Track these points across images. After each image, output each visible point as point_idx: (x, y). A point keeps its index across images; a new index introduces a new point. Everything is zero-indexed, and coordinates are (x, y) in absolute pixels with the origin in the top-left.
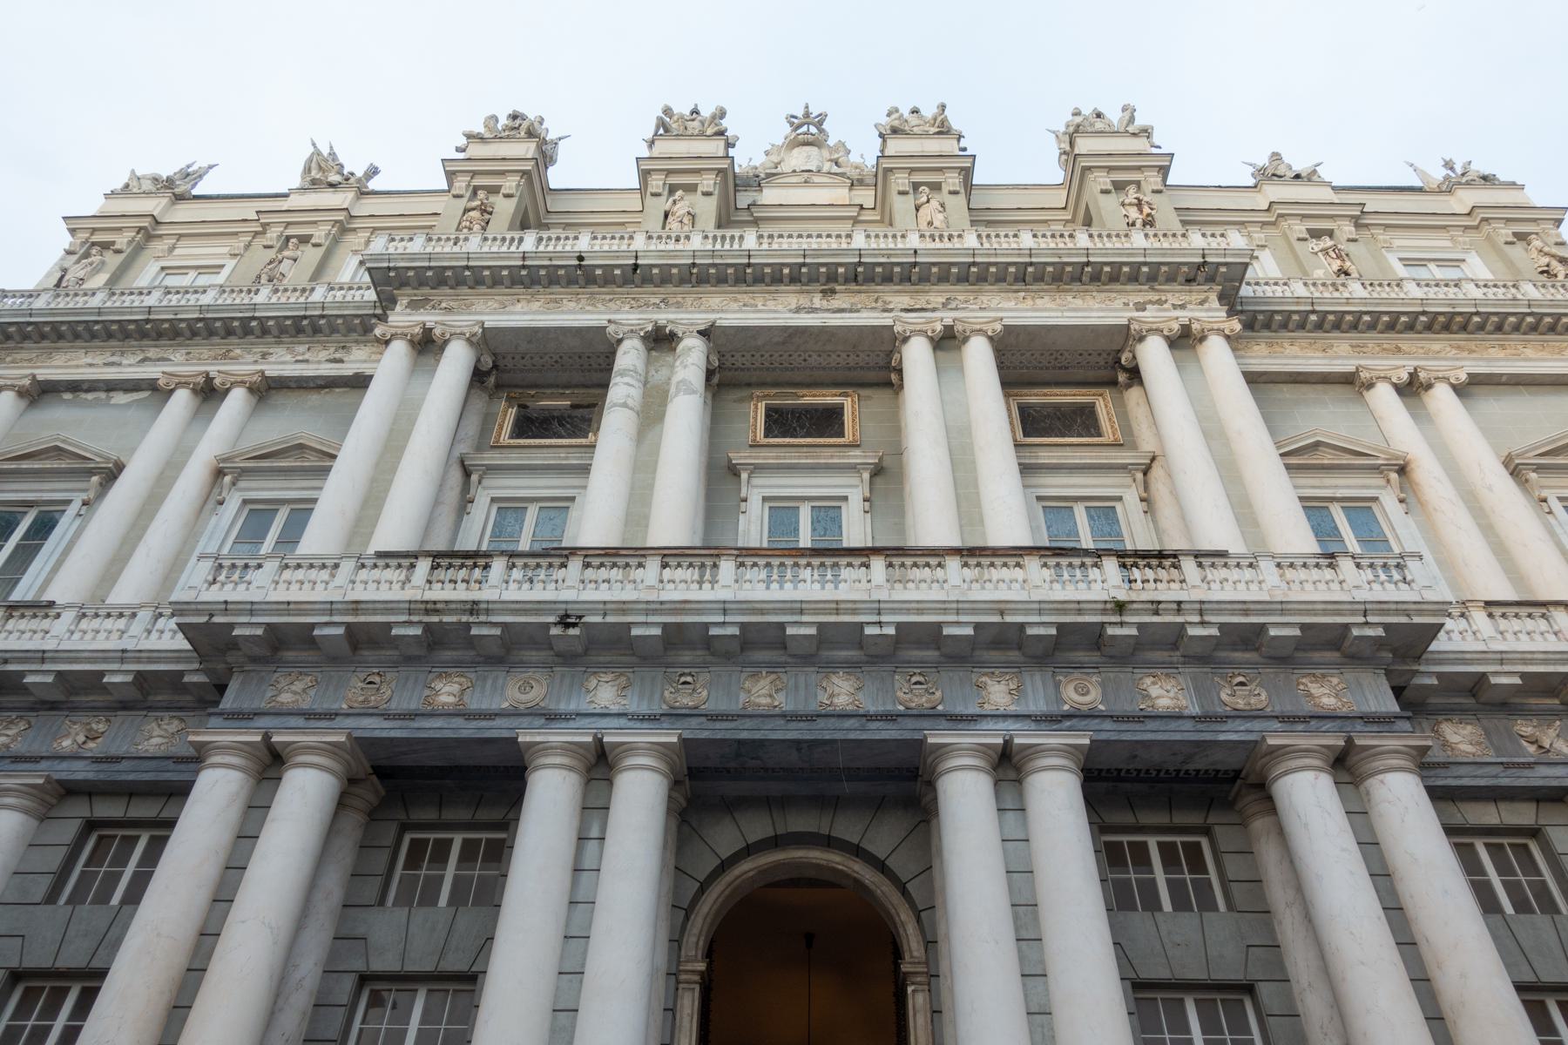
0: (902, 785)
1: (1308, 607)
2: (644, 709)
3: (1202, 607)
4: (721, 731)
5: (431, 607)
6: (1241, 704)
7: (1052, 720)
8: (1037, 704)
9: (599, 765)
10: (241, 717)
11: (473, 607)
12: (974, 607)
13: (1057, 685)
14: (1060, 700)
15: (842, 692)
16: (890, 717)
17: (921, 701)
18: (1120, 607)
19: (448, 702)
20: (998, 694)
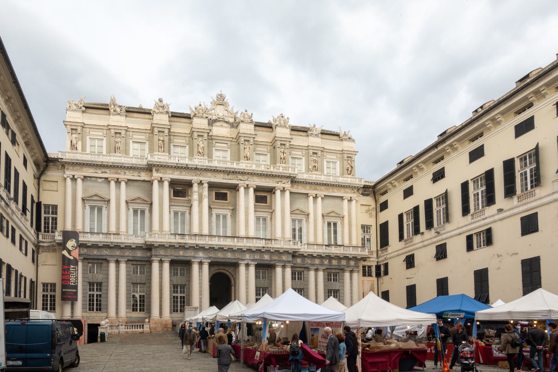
0: (235, 265)
2: (205, 256)
3: (273, 248)
4: (215, 260)
5: (180, 243)
7: (253, 260)
8: (252, 258)
9: (201, 263)
10: (156, 256)
11: (185, 243)
12: (247, 247)
15: (229, 255)
16: (235, 259)
17: (239, 257)
18: (264, 247)
19: (182, 254)
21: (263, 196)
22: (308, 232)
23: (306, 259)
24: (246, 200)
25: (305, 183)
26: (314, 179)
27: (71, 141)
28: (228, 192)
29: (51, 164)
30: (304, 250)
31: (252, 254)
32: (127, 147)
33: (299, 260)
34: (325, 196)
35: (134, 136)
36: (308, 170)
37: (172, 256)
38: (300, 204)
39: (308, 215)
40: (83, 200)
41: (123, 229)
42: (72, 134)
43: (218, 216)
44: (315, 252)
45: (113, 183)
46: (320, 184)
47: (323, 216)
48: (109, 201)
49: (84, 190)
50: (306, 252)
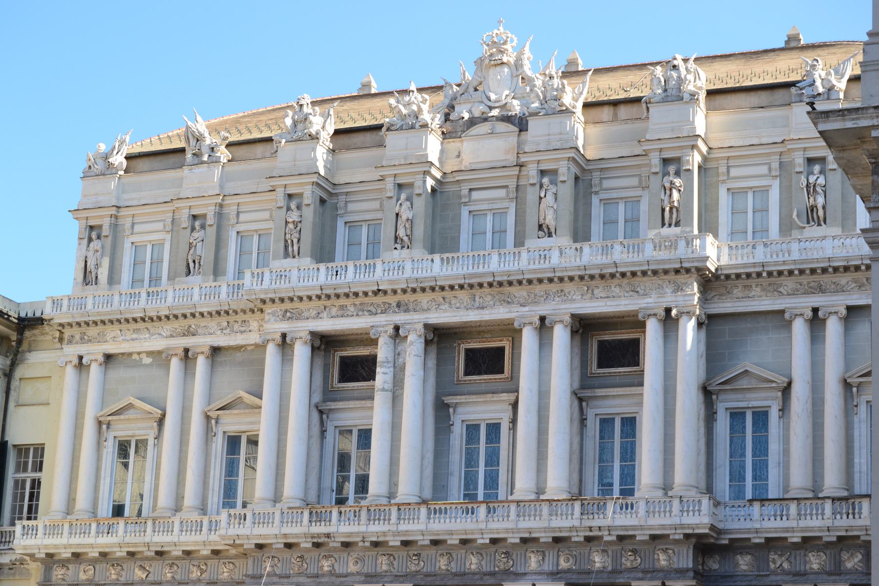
1: (651, 528)
3: (610, 529)
6: (629, 565)
8: (547, 567)
11: (328, 536)
13: (558, 556)
14: (558, 565)
16: (492, 574)
20: (533, 562)
21: (609, 348)
22: (786, 452)
23: (772, 556)
24: (547, 370)
25: (769, 277)
26: (796, 256)
27: (86, 262)
28: (506, 344)
29: (27, 333)
30: (748, 525)
31: (550, 555)
32: (222, 252)
33: (744, 563)
34: (850, 309)
35: (243, 217)
36: (786, 227)
37: (300, 574)
38: (755, 357)
39: (787, 390)
40: (100, 423)
41: (190, 498)
42: (90, 240)
43: (472, 430)
44: (792, 530)
45: (175, 364)
46: (824, 270)
47: (847, 385)
48: (161, 422)
49: (105, 395)
50: (757, 531)
